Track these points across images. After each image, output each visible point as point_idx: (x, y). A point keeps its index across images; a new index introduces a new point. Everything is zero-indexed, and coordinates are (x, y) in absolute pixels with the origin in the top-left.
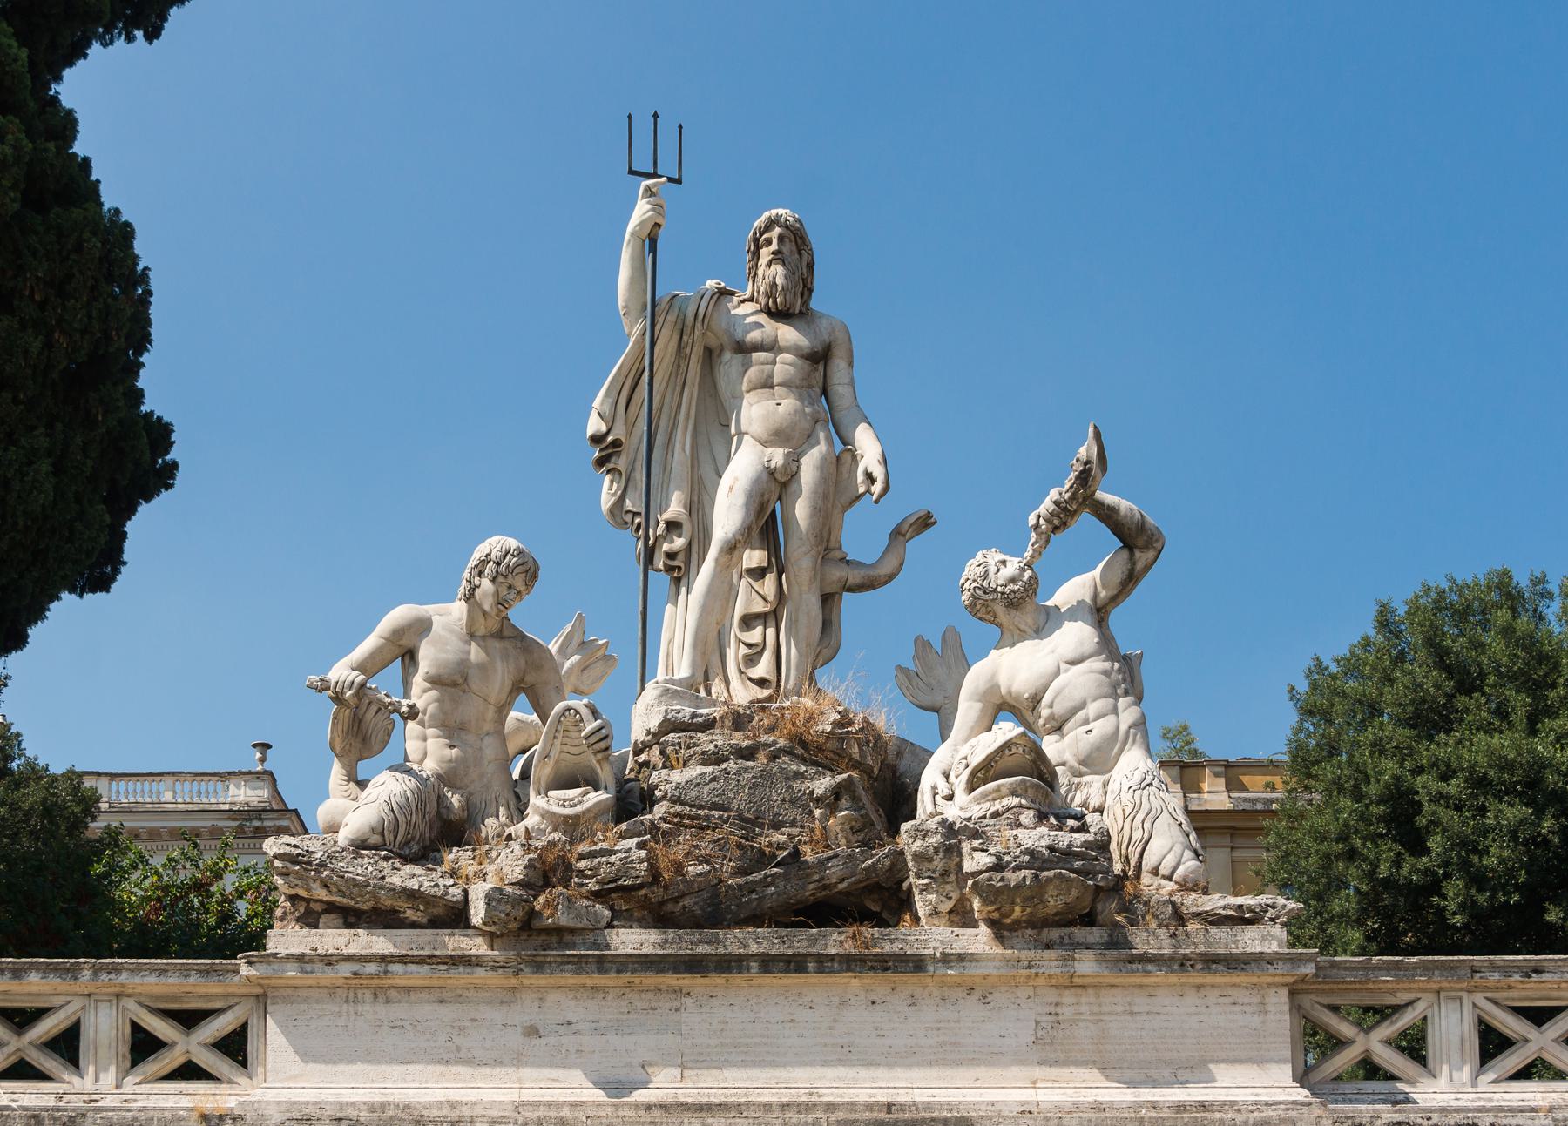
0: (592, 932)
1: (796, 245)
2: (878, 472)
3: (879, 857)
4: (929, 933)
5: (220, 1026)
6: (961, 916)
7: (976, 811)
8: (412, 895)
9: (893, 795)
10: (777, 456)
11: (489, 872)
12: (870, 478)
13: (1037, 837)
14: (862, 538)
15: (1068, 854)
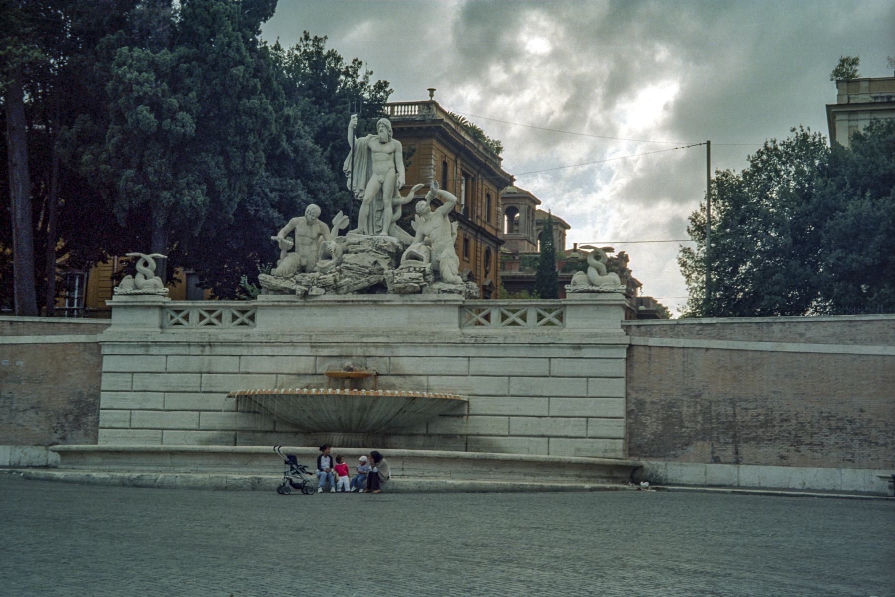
5: (249, 314)
8: (286, 288)
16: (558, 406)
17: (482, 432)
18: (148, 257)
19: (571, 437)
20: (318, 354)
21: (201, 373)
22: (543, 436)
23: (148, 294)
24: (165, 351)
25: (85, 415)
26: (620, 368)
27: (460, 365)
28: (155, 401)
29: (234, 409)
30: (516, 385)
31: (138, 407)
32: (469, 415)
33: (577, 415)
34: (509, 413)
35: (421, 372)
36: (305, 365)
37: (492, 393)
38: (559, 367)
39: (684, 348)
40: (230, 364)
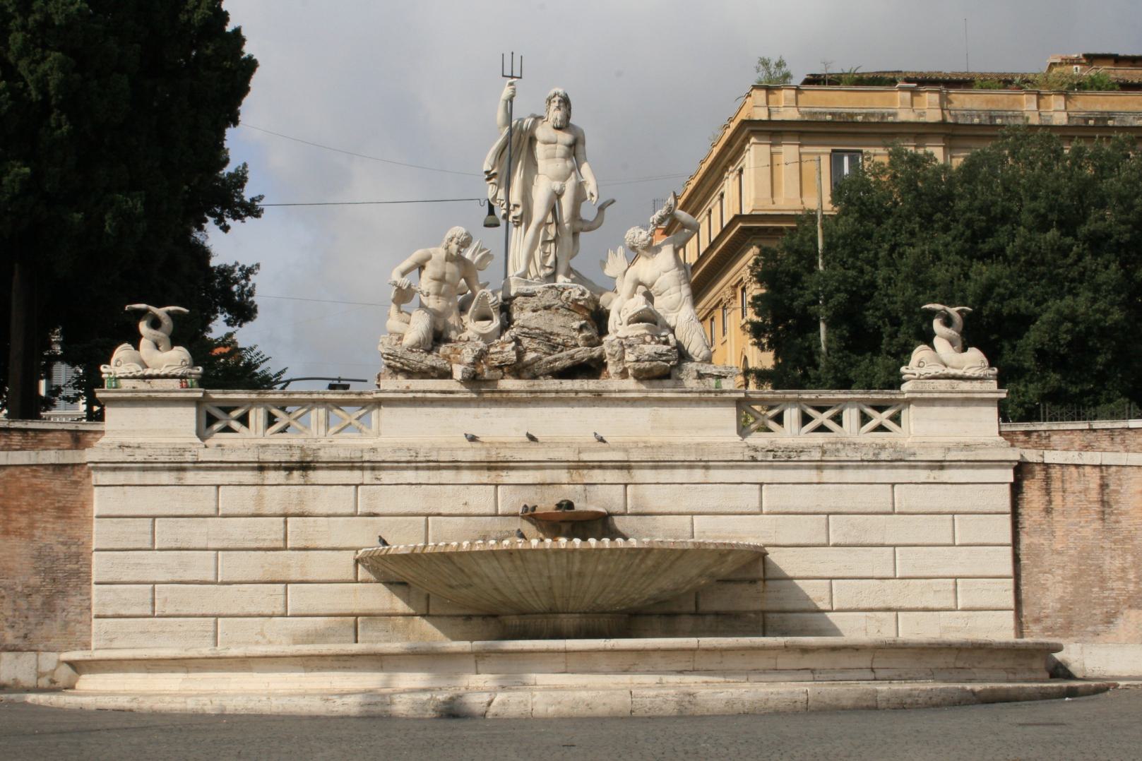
0: (493, 381)
1: (565, 102)
2: (595, 194)
3: (596, 352)
4: (611, 382)
6: (624, 374)
7: (630, 333)
9: (599, 319)
10: (557, 186)
11: (461, 361)
12: (592, 195)
13: (651, 348)
14: (588, 212)
15: (661, 355)
16: (908, 561)
17: (789, 606)
18: (161, 312)
19: (933, 610)
20: (499, 480)
21: (286, 516)
22: (889, 610)
23: (158, 377)
24: (216, 477)
25: (64, 593)
26: (1002, 499)
27: (748, 498)
28: (201, 565)
29: (351, 577)
30: (840, 529)
31: (169, 578)
32: (765, 580)
33: (941, 574)
34: (831, 575)
35: (684, 510)
36: (481, 499)
37: (803, 542)
38: (907, 498)
39: (1101, 466)
40: (340, 499)
